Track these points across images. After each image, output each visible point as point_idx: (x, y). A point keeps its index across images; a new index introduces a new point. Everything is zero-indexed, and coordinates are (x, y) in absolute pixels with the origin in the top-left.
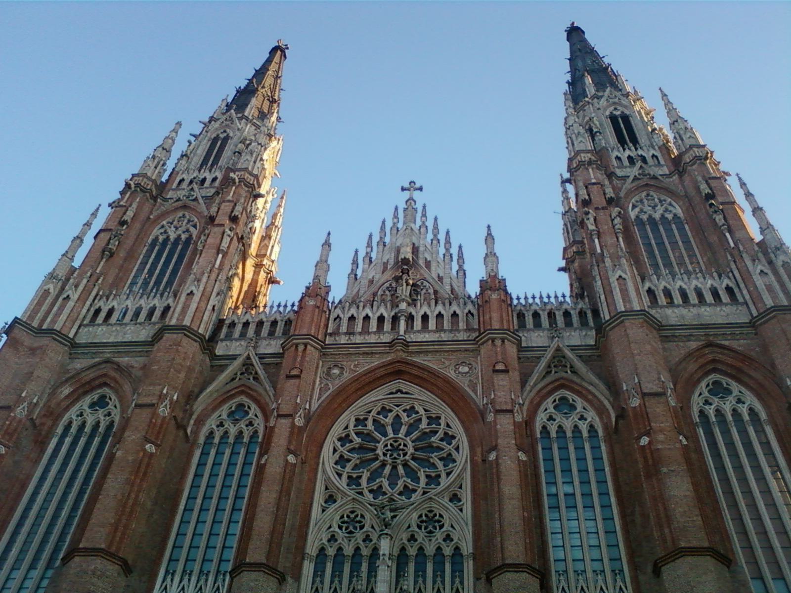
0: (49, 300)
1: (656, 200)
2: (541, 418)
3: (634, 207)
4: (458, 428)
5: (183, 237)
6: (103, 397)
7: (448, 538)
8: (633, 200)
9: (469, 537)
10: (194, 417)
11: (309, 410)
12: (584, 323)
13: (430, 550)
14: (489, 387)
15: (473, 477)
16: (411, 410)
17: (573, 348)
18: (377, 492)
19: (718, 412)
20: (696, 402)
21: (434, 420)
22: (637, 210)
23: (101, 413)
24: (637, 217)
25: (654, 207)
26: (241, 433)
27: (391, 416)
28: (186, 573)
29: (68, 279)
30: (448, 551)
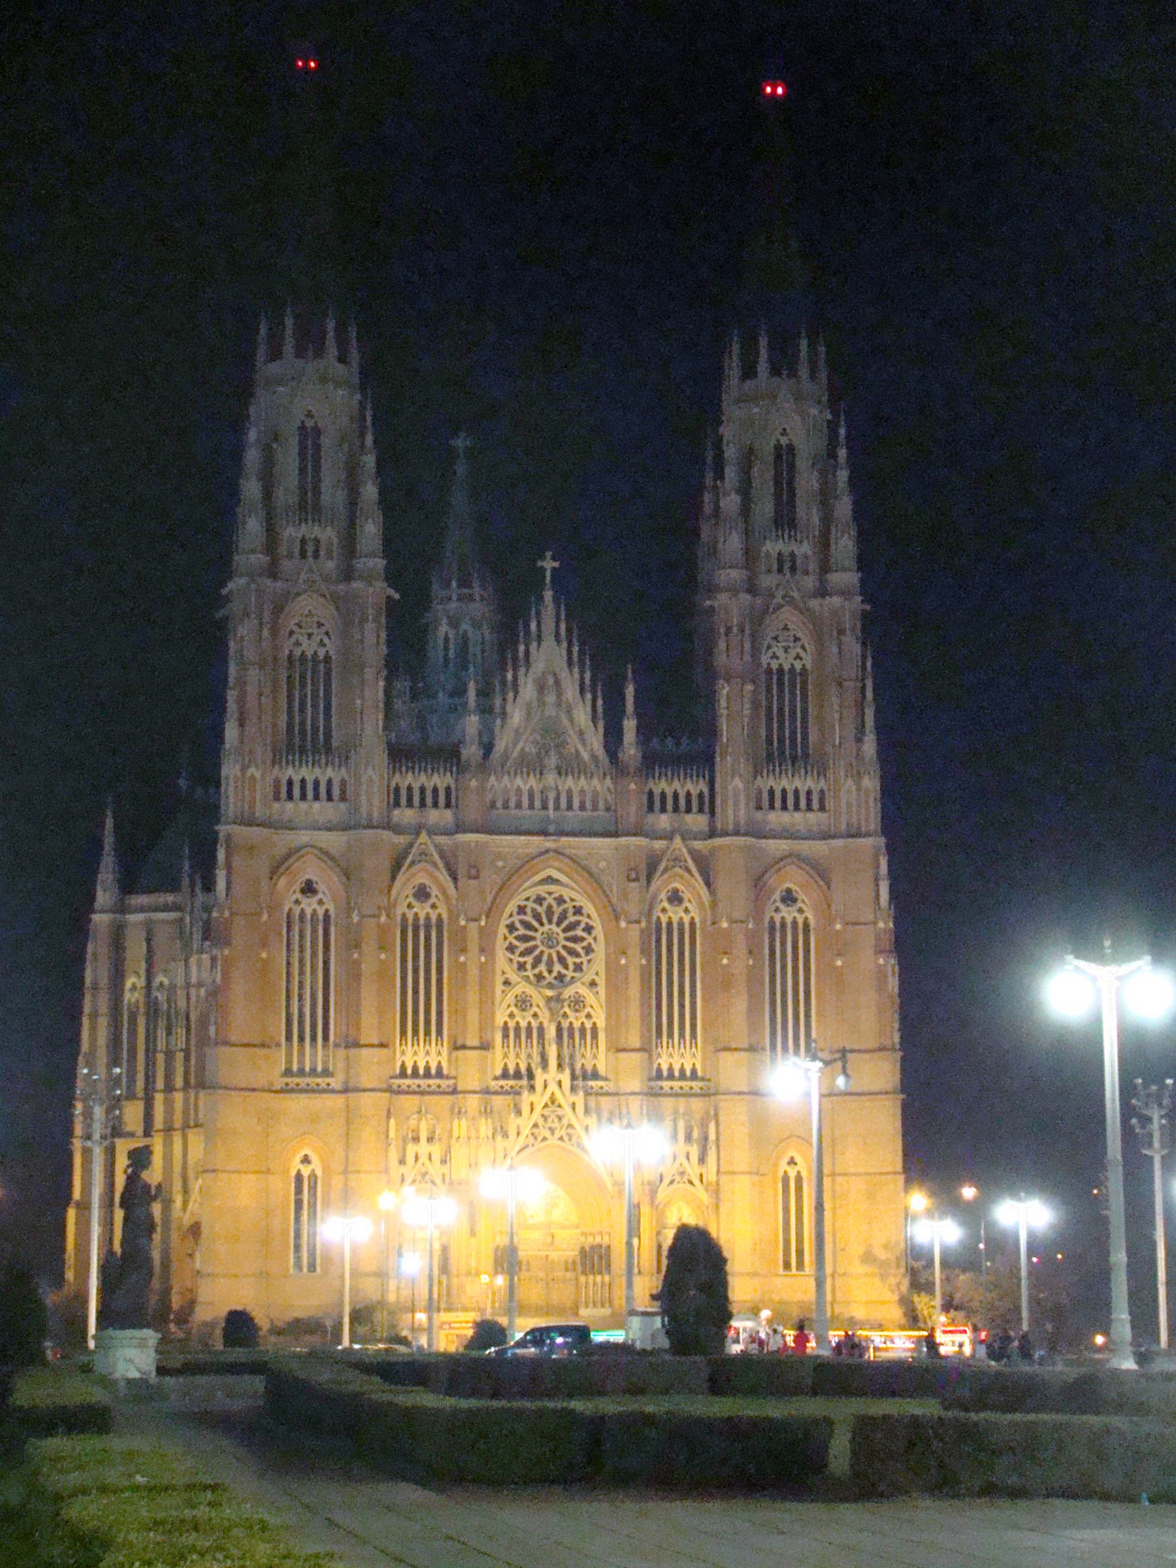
3: (769, 647)
4: (596, 922)
7: (589, 1016)
8: (769, 639)
12: (701, 811)
14: (624, 895)
16: (560, 900)
22: (770, 654)
23: (315, 899)
24: (769, 664)
25: (786, 650)
30: (588, 1025)
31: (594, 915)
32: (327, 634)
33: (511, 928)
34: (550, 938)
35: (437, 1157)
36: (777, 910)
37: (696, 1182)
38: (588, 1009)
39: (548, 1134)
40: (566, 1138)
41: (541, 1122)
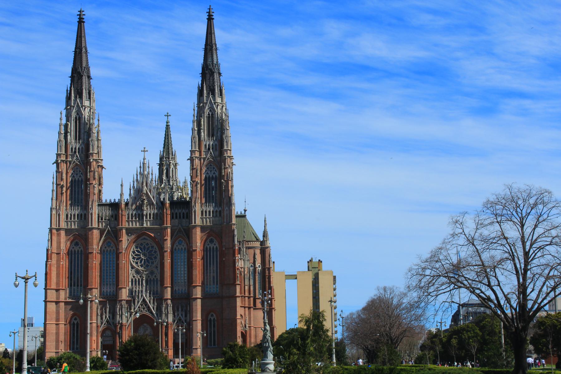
1: (212, 168)
2: (175, 246)
5: (80, 179)
6: (77, 242)
7: (155, 276)
9: (159, 276)
13: (152, 279)
15: (160, 263)
16: (147, 244)
19: (210, 247)
20: (206, 245)
21: (152, 247)
23: (78, 247)
25: (211, 171)
26: (110, 250)
27: (143, 245)
28: (107, 284)
29: (56, 207)
30: (155, 279)
31: (157, 248)
32: (82, 174)
33: (134, 252)
35: (111, 317)
36: (208, 245)
38: (155, 274)
41: (141, 306)
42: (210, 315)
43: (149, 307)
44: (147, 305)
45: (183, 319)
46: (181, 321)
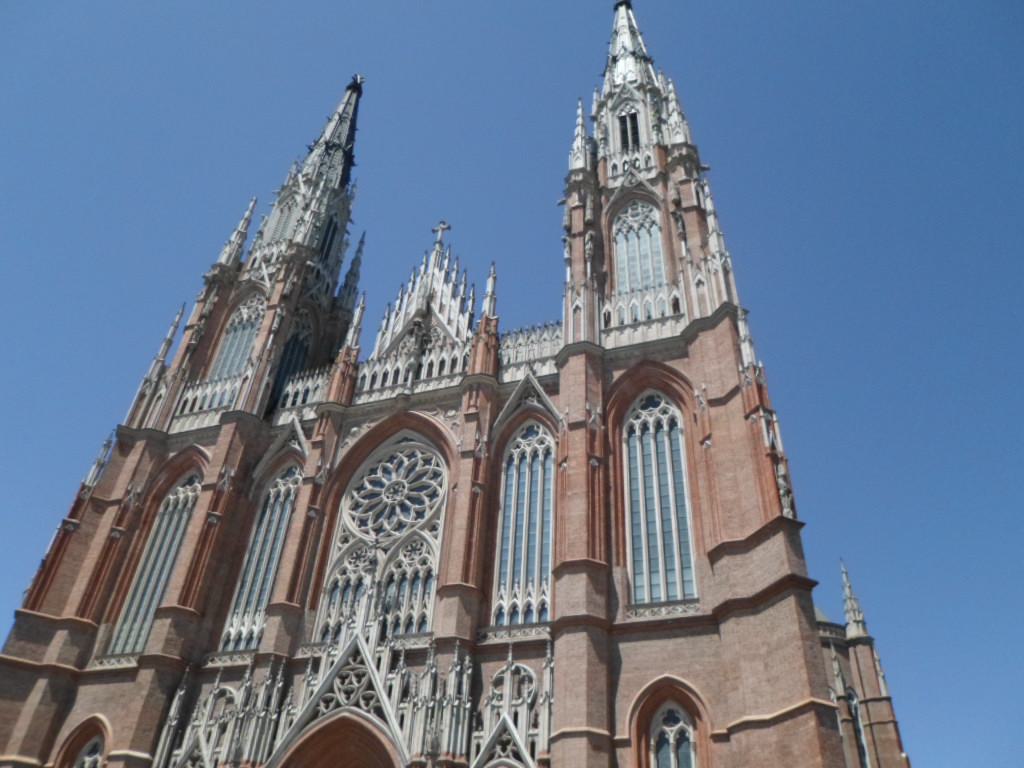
0: (146, 400)
7: (424, 562)
10: (255, 483)
11: (330, 470)
13: (409, 571)
17: (541, 379)
18: (378, 530)
34: (396, 492)
37: (526, 754)
39: (341, 697)
40: (362, 703)
41: (337, 681)
42: (659, 716)
43: (370, 686)
44: (364, 675)
45: (519, 736)
46: (509, 748)
